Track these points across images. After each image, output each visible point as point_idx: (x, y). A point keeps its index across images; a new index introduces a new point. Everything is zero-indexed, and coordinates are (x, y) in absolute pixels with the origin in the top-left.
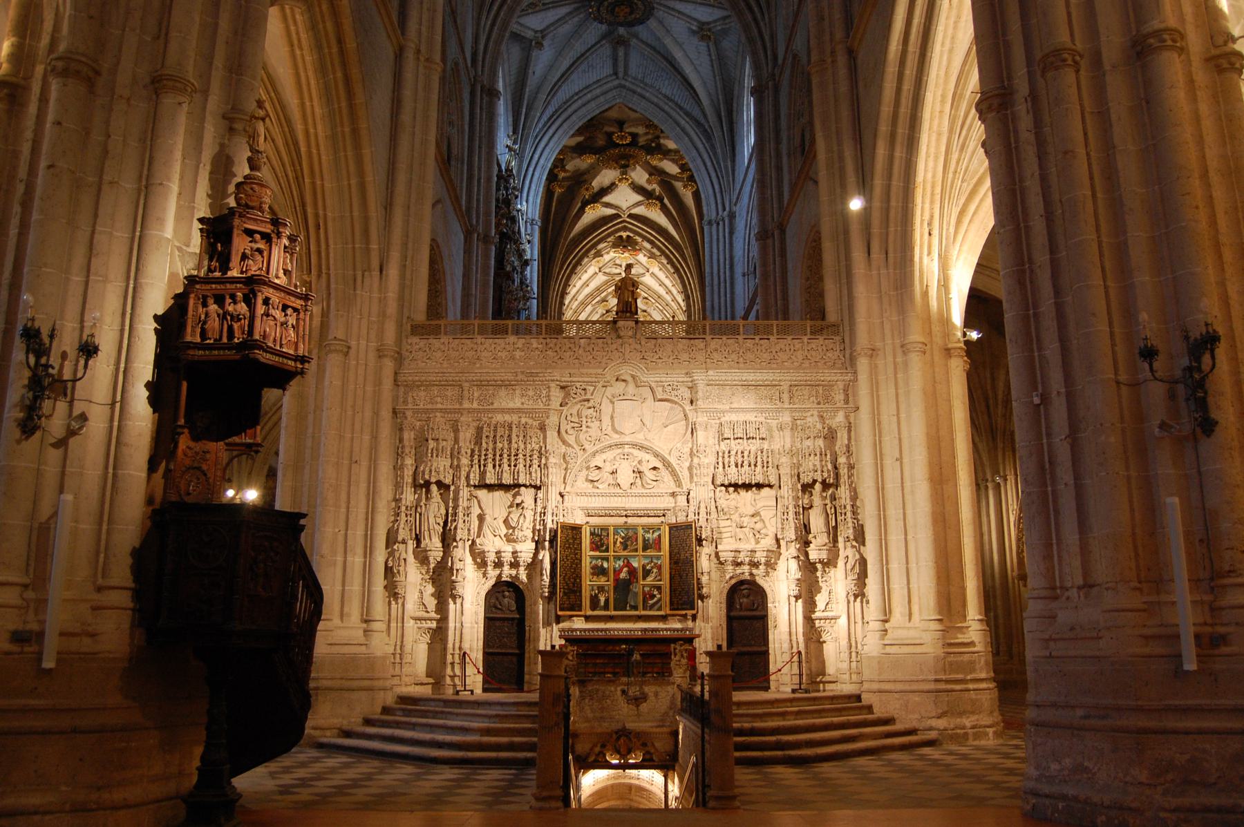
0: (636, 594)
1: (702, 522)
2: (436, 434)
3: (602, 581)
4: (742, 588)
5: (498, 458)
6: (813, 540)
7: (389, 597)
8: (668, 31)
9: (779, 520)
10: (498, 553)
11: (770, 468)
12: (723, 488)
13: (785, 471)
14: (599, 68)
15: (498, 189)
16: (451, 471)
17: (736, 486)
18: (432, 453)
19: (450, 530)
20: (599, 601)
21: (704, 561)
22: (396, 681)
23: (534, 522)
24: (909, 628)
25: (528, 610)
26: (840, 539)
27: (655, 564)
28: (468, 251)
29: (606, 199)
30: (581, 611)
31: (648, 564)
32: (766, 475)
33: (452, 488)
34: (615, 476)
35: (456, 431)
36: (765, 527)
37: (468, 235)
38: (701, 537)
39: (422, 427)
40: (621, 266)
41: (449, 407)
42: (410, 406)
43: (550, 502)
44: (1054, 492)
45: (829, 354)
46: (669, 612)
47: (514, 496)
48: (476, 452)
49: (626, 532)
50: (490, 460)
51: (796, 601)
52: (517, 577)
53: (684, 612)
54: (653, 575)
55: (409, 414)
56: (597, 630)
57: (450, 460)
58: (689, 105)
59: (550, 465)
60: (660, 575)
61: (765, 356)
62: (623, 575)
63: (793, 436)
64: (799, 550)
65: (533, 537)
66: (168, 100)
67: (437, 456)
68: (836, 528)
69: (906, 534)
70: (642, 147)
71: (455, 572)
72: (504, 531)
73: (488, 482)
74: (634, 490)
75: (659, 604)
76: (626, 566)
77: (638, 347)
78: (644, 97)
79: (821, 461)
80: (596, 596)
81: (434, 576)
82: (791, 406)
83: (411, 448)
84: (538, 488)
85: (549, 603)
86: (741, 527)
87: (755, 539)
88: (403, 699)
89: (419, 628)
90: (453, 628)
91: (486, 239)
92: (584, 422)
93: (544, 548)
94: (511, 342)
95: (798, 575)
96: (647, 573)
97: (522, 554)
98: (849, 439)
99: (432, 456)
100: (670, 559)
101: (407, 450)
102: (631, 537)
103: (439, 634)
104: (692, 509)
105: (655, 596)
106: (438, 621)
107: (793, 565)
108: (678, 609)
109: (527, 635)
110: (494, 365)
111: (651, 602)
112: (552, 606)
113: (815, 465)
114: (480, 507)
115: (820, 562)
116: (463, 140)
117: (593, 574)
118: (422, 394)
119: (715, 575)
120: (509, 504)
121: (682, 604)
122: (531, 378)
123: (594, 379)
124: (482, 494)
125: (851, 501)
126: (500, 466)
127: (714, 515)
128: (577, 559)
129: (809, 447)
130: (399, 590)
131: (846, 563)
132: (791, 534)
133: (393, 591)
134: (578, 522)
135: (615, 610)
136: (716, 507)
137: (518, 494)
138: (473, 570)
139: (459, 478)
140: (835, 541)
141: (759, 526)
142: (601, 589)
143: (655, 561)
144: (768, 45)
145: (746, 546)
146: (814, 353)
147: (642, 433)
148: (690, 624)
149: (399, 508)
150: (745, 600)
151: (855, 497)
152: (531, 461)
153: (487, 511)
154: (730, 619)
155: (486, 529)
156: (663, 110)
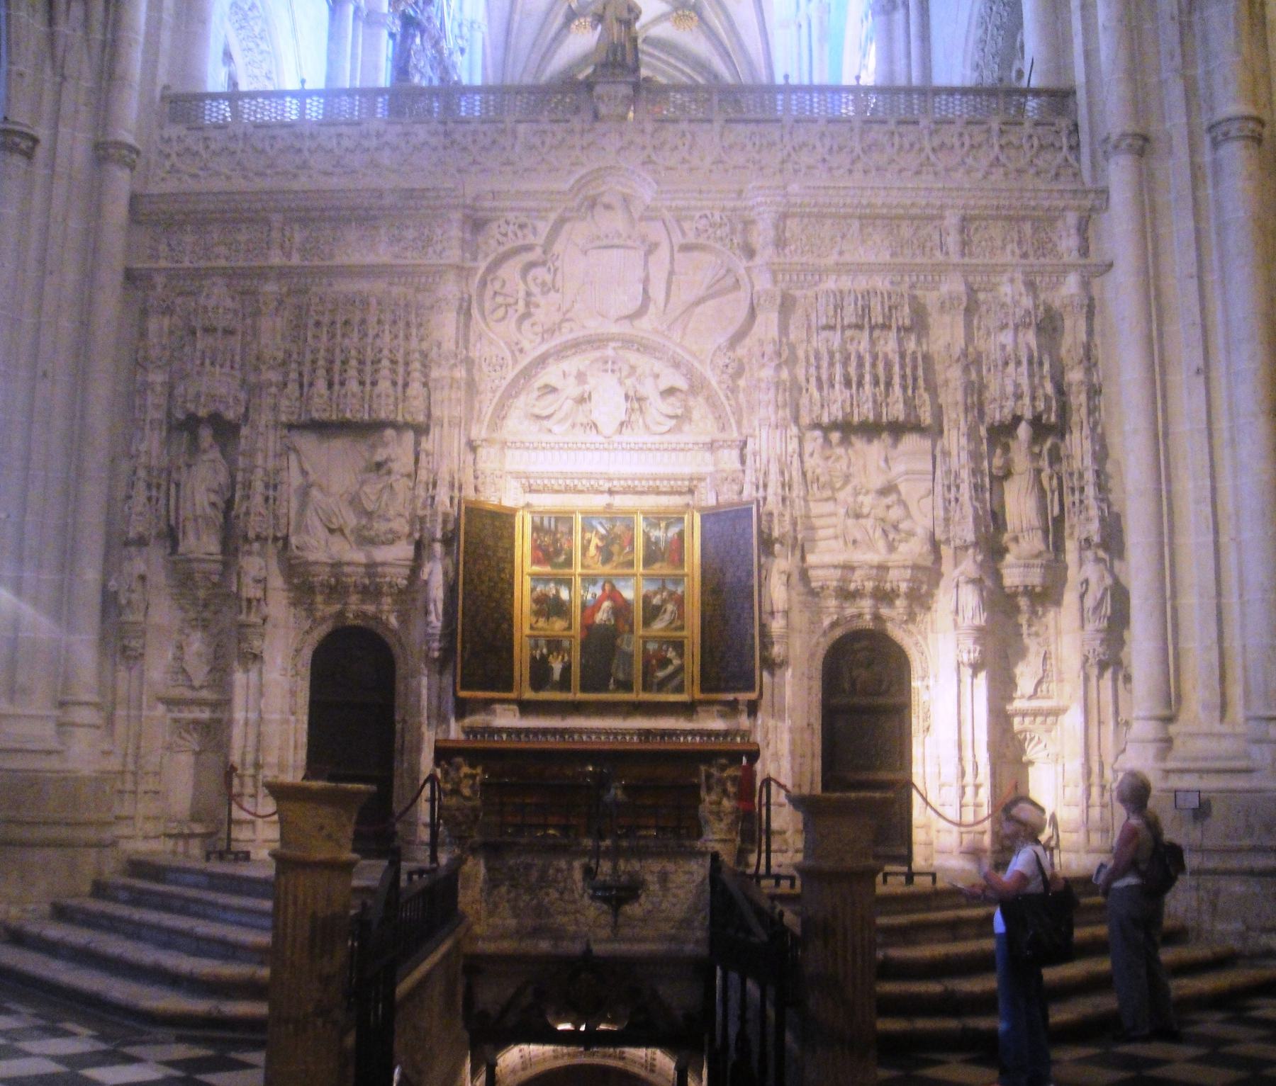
0: (630, 656)
1: (773, 504)
5: (337, 367)
6: (1012, 546)
9: (940, 502)
11: (922, 390)
12: (818, 433)
13: (952, 396)
16: (242, 396)
19: (237, 517)
21: (777, 592)
22: (122, 830)
24: (1221, 736)
25: (400, 687)
26: (1071, 546)
27: (671, 594)
30: (508, 687)
31: (655, 594)
32: (909, 404)
33: (245, 431)
34: (586, 406)
36: (908, 515)
38: (770, 535)
42: (163, 263)
46: (698, 695)
47: (373, 447)
49: (608, 526)
50: (321, 372)
51: (974, 675)
53: (730, 697)
54: (667, 617)
55: (160, 280)
56: (545, 732)
63: (968, 326)
64: (981, 566)
65: (410, 535)
68: (1059, 521)
69: (1216, 531)
72: (351, 520)
73: (316, 415)
74: (628, 437)
75: (676, 682)
79: (1031, 375)
81: (207, 615)
82: (967, 260)
84: (421, 430)
85: (441, 673)
88: (138, 867)
89: (176, 721)
90: (242, 722)
93: (432, 557)
95: (981, 620)
97: (388, 570)
98: (1090, 332)
99: (202, 364)
102: (619, 537)
104: (750, 477)
105: (668, 662)
107: (970, 598)
111: (661, 674)
112: (447, 680)
113: (1017, 386)
114: (304, 473)
115: (1029, 592)
117: (538, 613)
118: (189, 238)
119: (799, 619)
120: (362, 464)
122: (412, 203)
124: (307, 442)
127: (798, 491)
129: (1003, 347)
132: (967, 532)
134: (508, 502)
135: (584, 688)
136: (804, 474)
138: (285, 602)
140: (1059, 547)
141: (896, 513)
142: (555, 645)
143: (671, 587)
146: (1013, 152)
151: (1101, 454)
153: (313, 477)
155: (313, 521)
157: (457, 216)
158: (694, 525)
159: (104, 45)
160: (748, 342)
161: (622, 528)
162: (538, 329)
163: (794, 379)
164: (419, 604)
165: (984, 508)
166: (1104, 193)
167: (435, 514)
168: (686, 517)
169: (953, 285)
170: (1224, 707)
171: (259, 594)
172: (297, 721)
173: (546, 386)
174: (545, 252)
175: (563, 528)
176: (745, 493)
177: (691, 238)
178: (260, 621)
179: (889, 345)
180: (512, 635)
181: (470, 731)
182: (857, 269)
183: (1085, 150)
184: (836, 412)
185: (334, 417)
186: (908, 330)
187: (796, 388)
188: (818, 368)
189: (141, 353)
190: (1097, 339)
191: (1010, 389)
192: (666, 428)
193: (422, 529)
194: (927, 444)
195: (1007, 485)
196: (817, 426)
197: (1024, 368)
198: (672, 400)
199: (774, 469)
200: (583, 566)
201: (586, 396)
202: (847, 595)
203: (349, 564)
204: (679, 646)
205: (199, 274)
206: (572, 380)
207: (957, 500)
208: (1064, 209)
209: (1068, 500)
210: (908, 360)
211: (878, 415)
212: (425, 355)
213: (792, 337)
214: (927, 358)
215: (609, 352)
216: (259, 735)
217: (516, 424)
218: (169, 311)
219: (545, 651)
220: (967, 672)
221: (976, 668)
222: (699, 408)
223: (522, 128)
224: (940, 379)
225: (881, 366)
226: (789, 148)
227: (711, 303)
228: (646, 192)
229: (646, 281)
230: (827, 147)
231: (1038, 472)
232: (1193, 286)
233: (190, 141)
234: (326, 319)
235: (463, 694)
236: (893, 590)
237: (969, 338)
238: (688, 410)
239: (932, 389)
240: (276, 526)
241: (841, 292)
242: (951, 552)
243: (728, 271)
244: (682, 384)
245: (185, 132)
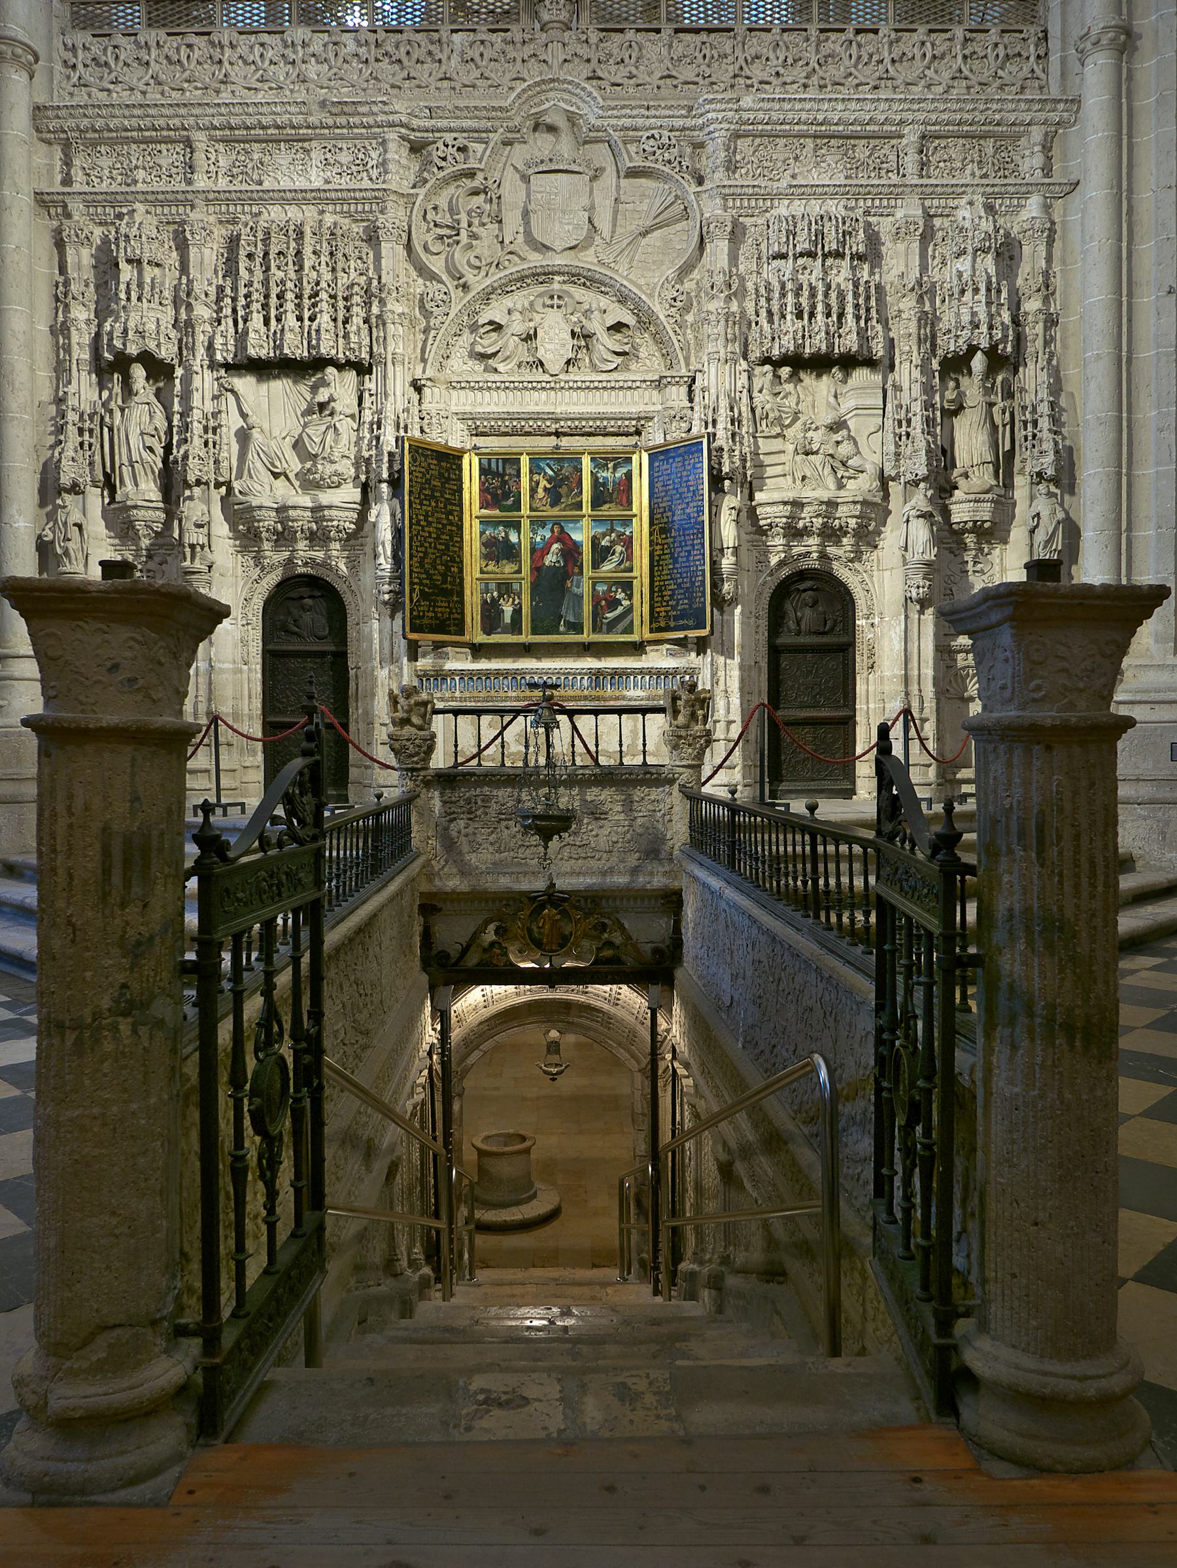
1: (722, 440)
2: (134, 249)
4: (802, 587)
5: (273, 301)
6: (962, 482)
11: (874, 322)
12: (768, 367)
13: (905, 328)
16: (173, 334)
18: (128, 293)
23: (357, 443)
25: (352, 633)
26: (1021, 483)
27: (620, 535)
31: (604, 535)
32: (863, 336)
33: (179, 372)
35: (182, 246)
36: (858, 453)
39: (106, 241)
42: (76, 187)
43: (391, 399)
45: (1011, 67)
46: (648, 636)
47: (314, 389)
48: (228, 291)
51: (921, 612)
52: (325, 565)
53: (680, 635)
54: (616, 558)
57: (170, 311)
59: (388, 317)
60: (630, 557)
61: (868, 70)
62: (550, 559)
64: (931, 500)
65: (357, 477)
67: (139, 299)
68: (1011, 454)
71: (188, 550)
72: (294, 465)
73: (252, 352)
74: (575, 375)
75: (626, 621)
76: (558, 540)
77: (583, 51)
79: (989, 303)
82: (925, 181)
83: (87, 285)
85: (392, 617)
86: (807, 454)
87: (836, 477)
92: (464, 224)
93: (378, 499)
94: (298, 42)
95: (931, 556)
96: (601, 554)
97: (334, 513)
98: (1049, 259)
99: (128, 299)
100: (651, 524)
102: (567, 478)
105: (618, 602)
107: (920, 532)
108: (667, 629)
109: (352, 685)
110: (261, 95)
112: (398, 621)
113: (974, 314)
114: (244, 416)
119: (747, 559)
120: (304, 406)
121: (676, 618)
122: (341, 120)
123: (484, 124)
124: (245, 384)
125: (1051, 394)
126: (279, 320)
128: (451, 524)
131: (1032, 532)
134: (455, 443)
136: (753, 410)
137: (324, 383)
138: (231, 550)
139: (193, 349)
140: (1009, 485)
141: (845, 449)
142: (506, 588)
146: (976, 65)
147: (592, 249)
150: (808, 612)
152: (348, 309)
153: (252, 420)
154: (775, 652)
158: (641, 464)
160: (696, 275)
161: (571, 469)
163: (743, 313)
164: (368, 549)
165: (935, 442)
166: (1077, 101)
167: (380, 454)
168: (635, 458)
169: (909, 209)
171: (202, 540)
172: (250, 669)
173: (491, 323)
176: (695, 431)
178: (205, 569)
179: (841, 274)
180: (462, 579)
183: (1055, 58)
184: (787, 344)
185: (272, 355)
186: (860, 257)
188: (768, 300)
189: (61, 288)
190: (1056, 268)
191: (966, 318)
192: (614, 365)
193: (367, 472)
194: (878, 378)
196: (766, 360)
197: (982, 296)
200: (532, 509)
201: (532, 332)
203: (294, 508)
204: (627, 586)
206: (516, 316)
207: (908, 435)
208: (1028, 124)
209: (1019, 434)
210: (861, 289)
211: (831, 346)
213: (742, 268)
214: (879, 288)
216: (210, 684)
219: (495, 594)
222: (646, 347)
224: (892, 312)
225: (833, 295)
226: (741, 61)
230: (782, 58)
233: (96, 50)
236: (841, 527)
237: (924, 268)
241: (793, 216)
242: (901, 487)
243: (677, 197)
244: (630, 319)
245: (90, 38)
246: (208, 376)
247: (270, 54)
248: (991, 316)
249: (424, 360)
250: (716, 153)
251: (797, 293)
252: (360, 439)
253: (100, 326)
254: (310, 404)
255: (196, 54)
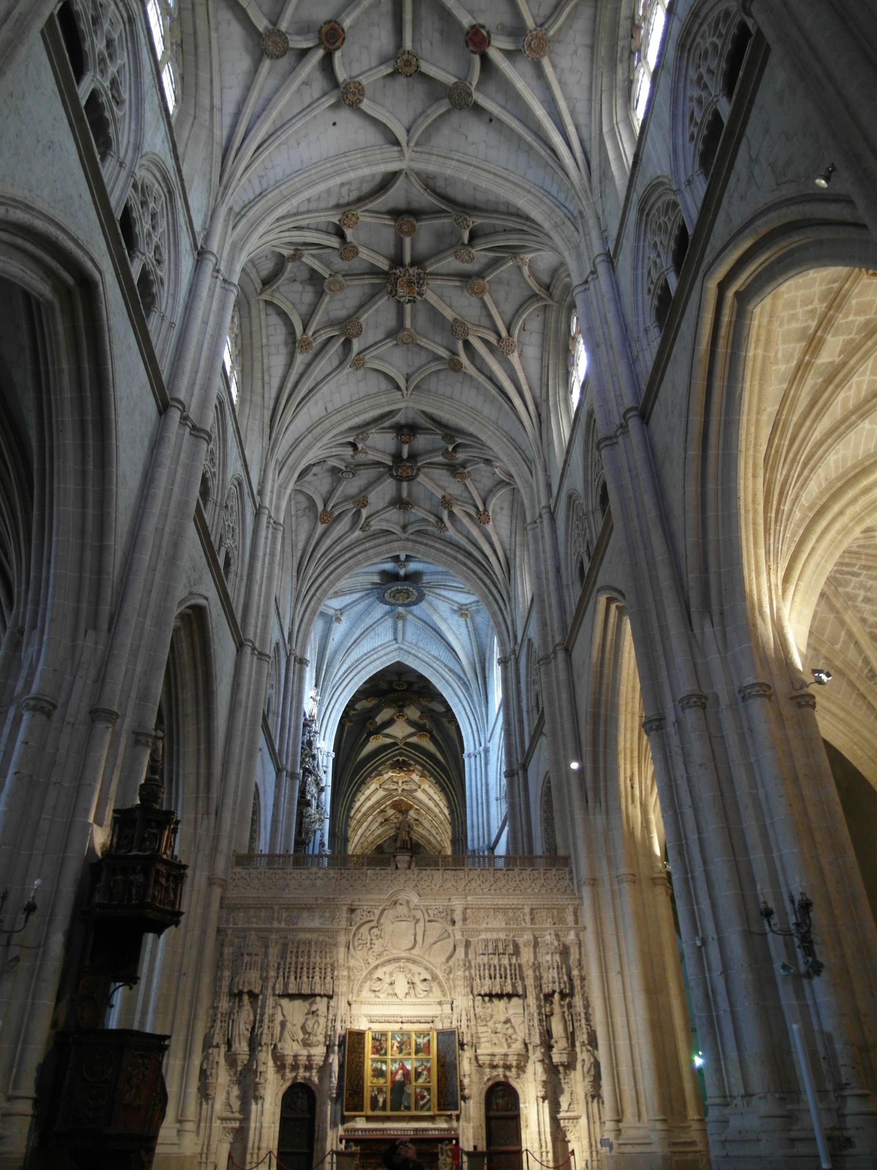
0: (409, 1095)
1: (464, 1029)
3: (382, 1081)
4: (498, 1089)
6: (555, 1045)
7: (201, 1098)
8: (435, 610)
9: (527, 1026)
10: (296, 1056)
12: (480, 998)
13: (530, 982)
14: (383, 635)
15: (304, 734)
16: (261, 982)
17: (491, 996)
20: (378, 1101)
21: (466, 1066)
25: (318, 1110)
26: (578, 1044)
28: (278, 786)
29: (387, 731)
30: (362, 1110)
32: (514, 986)
33: (261, 997)
35: (267, 947)
36: (515, 1032)
37: (279, 771)
40: (397, 783)
41: (263, 926)
42: (231, 925)
44: (717, 1016)
45: (562, 882)
46: (437, 1112)
47: (311, 1005)
50: (292, 973)
51: (543, 1102)
52: (310, 1079)
53: (449, 1113)
55: (229, 932)
56: (376, 1130)
57: (259, 973)
58: (452, 664)
59: (340, 977)
61: (511, 884)
63: (535, 953)
64: (543, 1054)
66: (100, 726)
68: (573, 1033)
69: (630, 1040)
70: (415, 692)
72: (301, 1036)
73: (290, 992)
74: (410, 999)
78: (417, 657)
79: (558, 974)
80: (376, 1096)
84: (330, 997)
86: (496, 1033)
89: (224, 1128)
91: (293, 776)
93: (333, 1052)
95: (544, 1078)
96: (418, 1075)
101: (226, 963)
103: (240, 1134)
104: (455, 1017)
106: (241, 1121)
107: (539, 1068)
111: (422, 1103)
112: (339, 1106)
113: (553, 977)
114: (284, 1016)
115: (562, 1065)
116: (279, 699)
117: (374, 1076)
118: (242, 915)
119: (475, 1078)
120: (306, 1011)
124: (285, 1002)
130: (210, 1092)
132: (537, 1040)
133: (205, 1093)
135: (392, 1110)
137: (314, 1002)
139: (267, 988)
140: (573, 1045)
141: (510, 1031)
142: (380, 1090)
144: (510, 628)
145: (500, 1050)
148: (454, 1124)
149: (216, 1015)
151: (587, 1006)
153: (289, 1018)
154: (489, 1119)
155: (287, 1036)
156: (432, 667)
157: (345, 908)
159: (214, 836)
160: (453, 959)
162: (375, 954)
163: (470, 974)
166: (581, 898)
169: (528, 937)
170: (639, 1115)
174: (378, 922)
175: (383, 1038)
177: (432, 918)
179: (505, 961)
181: (346, 1130)
182: (492, 930)
184: (485, 990)
186: (512, 955)
187: (472, 979)
190: (583, 957)
191: (551, 979)
194: (520, 1001)
195: (552, 1018)
198: (425, 983)
199: (464, 1013)
202: (494, 1067)
204: (428, 1090)
205: (244, 930)
206: (387, 976)
209: (576, 1024)
211: (502, 990)
212: (332, 965)
213: (470, 957)
214: (520, 966)
215: (402, 964)
217: (366, 994)
218: (232, 945)
220: (541, 1100)
221: (544, 1098)
222: (435, 985)
223: (369, 872)
224: (525, 975)
225: (503, 970)
227: (439, 943)
228: (415, 899)
229: (415, 935)
231: (564, 1012)
232: (614, 938)
234: (295, 950)
235: (346, 1113)
237: (535, 957)
238: (431, 987)
239: (522, 979)
240: (272, 1039)
244: (429, 977)
246: (272, 999)
247: (303, 877)
248: (559, 979)
249: (352, 993)
250: (458, 916)
251: (489, 970)
252: (327, 1026)
253: (232, 979)
254: (309, 1010)
255: (278, 876)
